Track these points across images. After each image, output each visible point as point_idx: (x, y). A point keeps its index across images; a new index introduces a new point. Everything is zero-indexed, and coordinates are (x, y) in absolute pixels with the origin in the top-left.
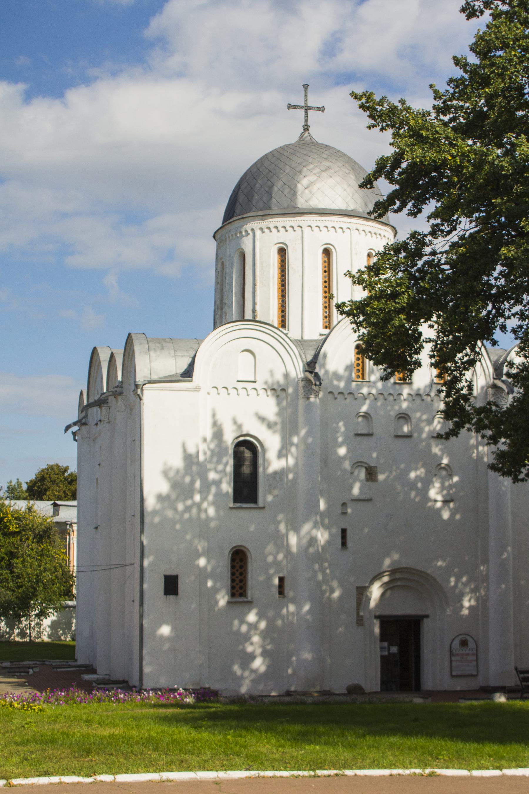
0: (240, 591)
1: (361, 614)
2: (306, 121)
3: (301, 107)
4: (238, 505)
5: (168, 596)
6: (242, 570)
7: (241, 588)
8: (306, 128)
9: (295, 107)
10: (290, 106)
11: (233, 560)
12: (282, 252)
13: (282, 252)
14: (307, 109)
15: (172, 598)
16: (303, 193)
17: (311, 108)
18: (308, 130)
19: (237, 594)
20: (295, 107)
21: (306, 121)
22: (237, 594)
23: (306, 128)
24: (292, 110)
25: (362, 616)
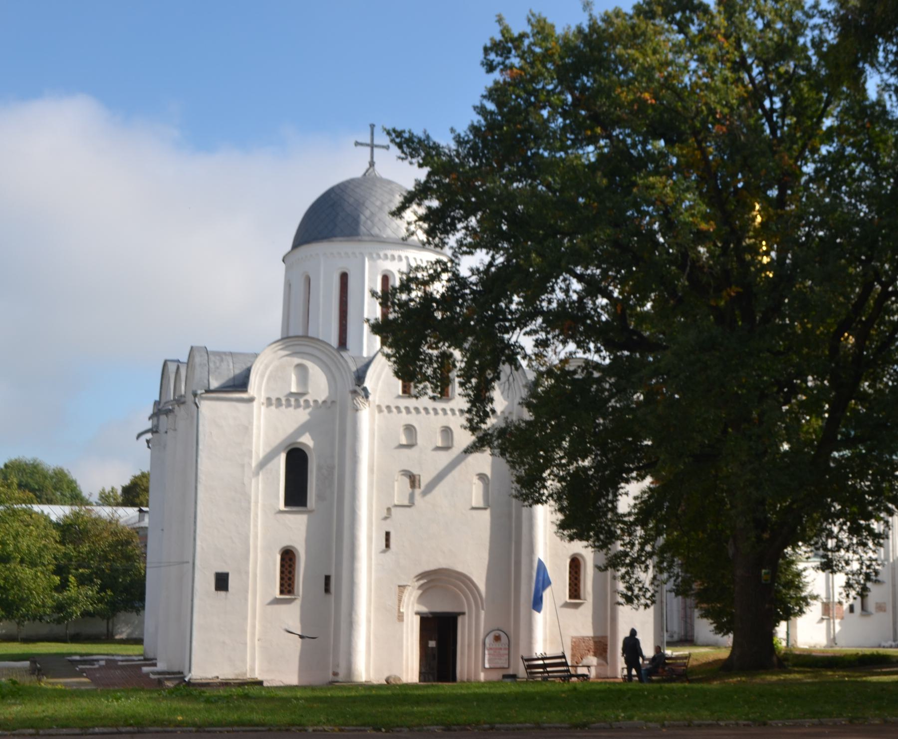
1: (401, 610)
2: (372, 157)
3: (367, 145)
5: (219, 592)
7: (290, 585)
8: (372, 164)
9: (362, 144)
10: (357, 144)
11: (283, 559)
14: (372, 146)
15: (222, 593)
16: (365, 222)
17: (377, 146)
18: (373, 165)
19: (286, 591)
20: (362, 144)
21: (372, 157)
23: (372, 164)
24: (359, 148)
25: (403, 613)
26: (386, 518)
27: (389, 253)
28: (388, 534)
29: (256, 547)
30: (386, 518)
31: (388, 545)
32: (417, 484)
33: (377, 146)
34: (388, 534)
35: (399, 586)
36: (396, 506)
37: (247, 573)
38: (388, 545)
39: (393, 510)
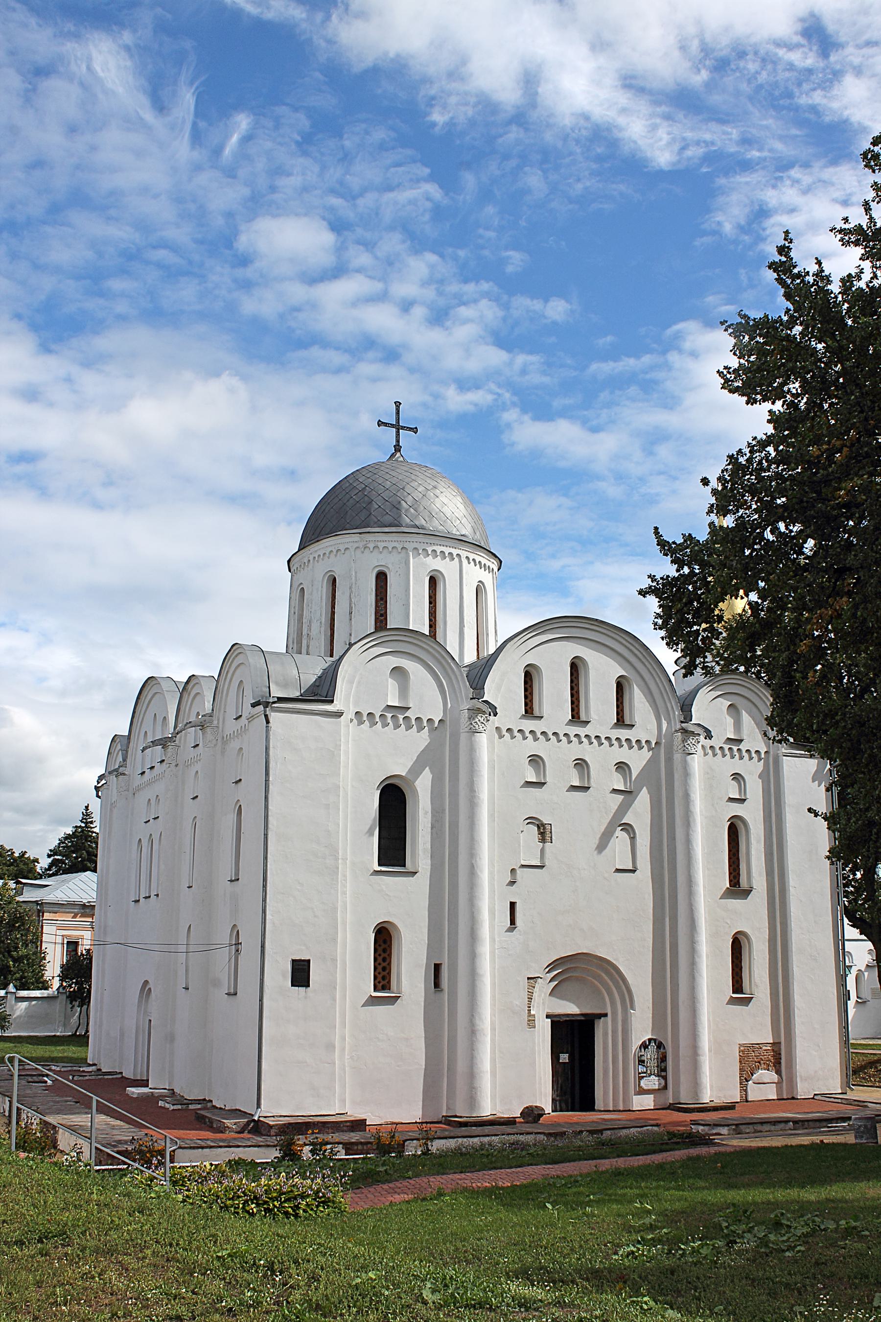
0: (383, 983)
1: (532, 1012)
2: (398, 441)
3: (392, 426)
4: (383, 869)
6: (386, 955)
8: (398, 448)
9: (386, 424)
10: (380, 423)
12: (381, 578)
13: (381, 578)
14: (398, 427)
15: (302, 989)
16: (407, 510)
17: (403, 428)
18: (400, 451)
20: (386, 424)
21: (398, 441)
22: (380, 986)
23: (398, 448)
26: (512, 883)
27: (439, 549)
28: (513, 905)
29: (344, 923)
30: (512, 883)
31: (513, 921)
32: (548, 835)
33: (403, 428)
34: (513, 905)
35: (528, 978)
36: (523, 866)
37: (334, 960)
38: (513, 921)
39: (519, 872)
